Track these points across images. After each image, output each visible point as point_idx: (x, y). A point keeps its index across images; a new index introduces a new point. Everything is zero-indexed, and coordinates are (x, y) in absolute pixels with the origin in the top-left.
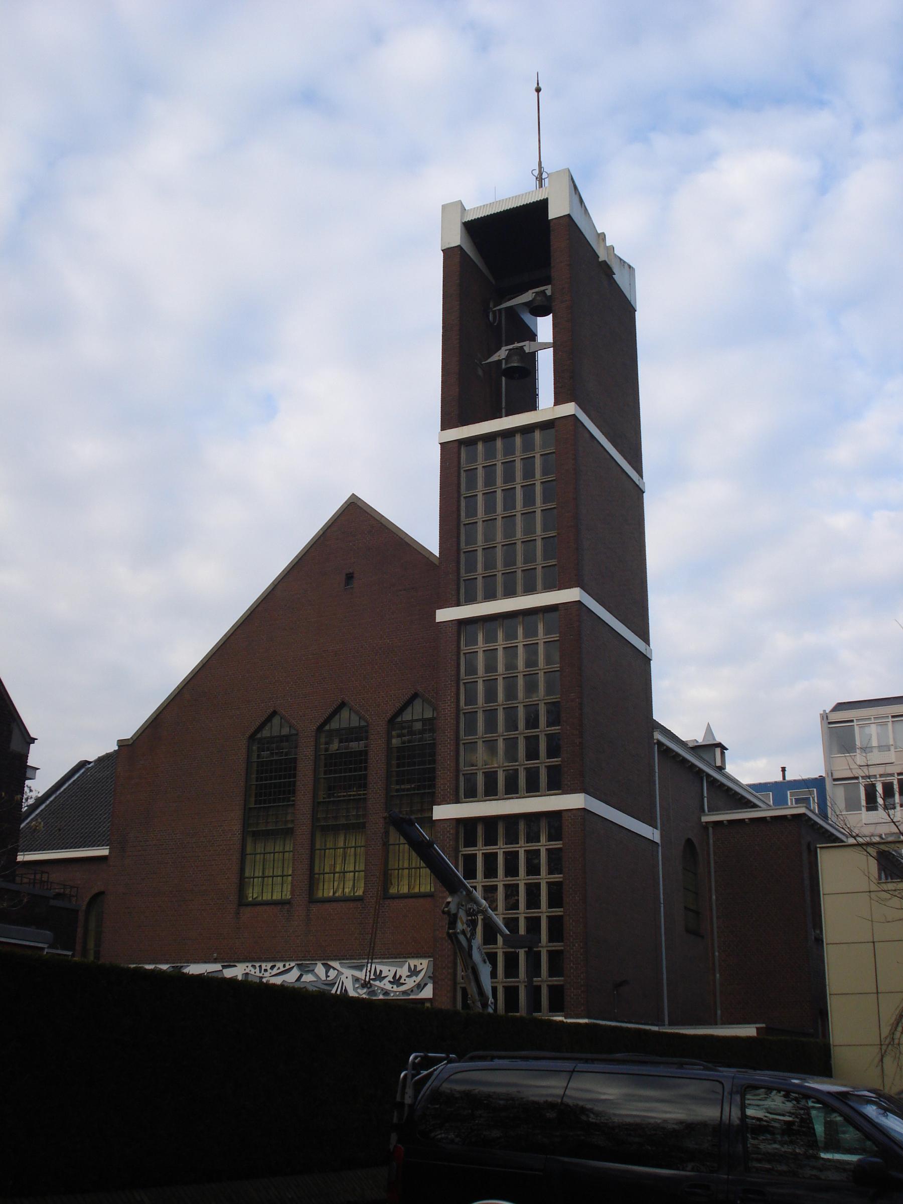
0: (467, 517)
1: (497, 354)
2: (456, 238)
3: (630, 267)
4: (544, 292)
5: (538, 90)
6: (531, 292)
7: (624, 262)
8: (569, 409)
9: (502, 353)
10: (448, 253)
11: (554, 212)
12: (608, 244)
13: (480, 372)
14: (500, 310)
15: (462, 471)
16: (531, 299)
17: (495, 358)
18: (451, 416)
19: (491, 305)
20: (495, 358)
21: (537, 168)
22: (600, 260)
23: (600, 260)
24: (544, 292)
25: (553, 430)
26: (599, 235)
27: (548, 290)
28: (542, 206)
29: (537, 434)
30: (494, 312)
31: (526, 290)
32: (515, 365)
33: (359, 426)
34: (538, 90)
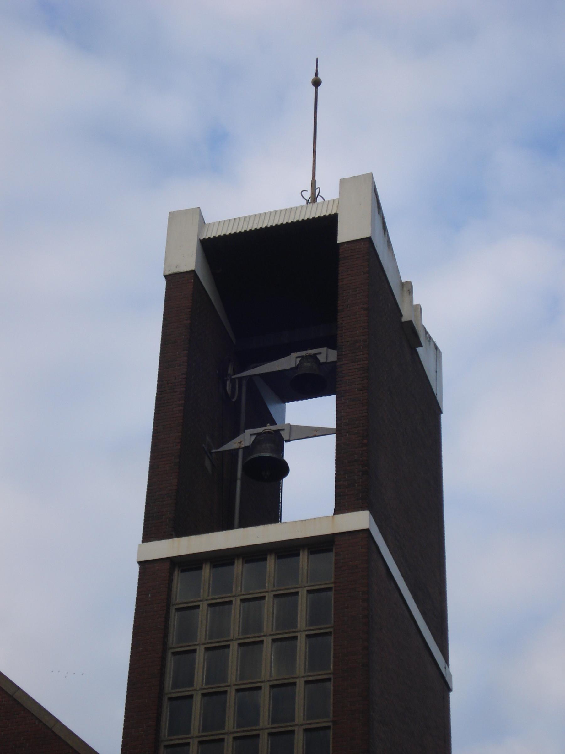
0: (175, 685)
1: (238, 439)
2: (189, 260)
3: (436, 348)
4: (314, 357)
5: (317, 83)
6: (294, 355)
7: (430, 338)
8: (360, 520)
9: (246, 438)
10: (172, 280)
11: (345, 234)
12: (415, 302)
13: (208, 464)
14: (240, 379)
15: (173, 611)
16: (293, 365)
17: (233, 445)
18: (156, 526)
19: (230, 371)
20: (233, 445)
21: (309, 188)
22: (404, 319)
23: (404, 319)
24: (314, 357)
25: (332, 556)
26: (403, 285)
27: (326, 355)
28: (330, 222)
29: (304, 558)
30: (233, 381)
31: (286, 353)
32: (268, 455)
33: (314, 76)
34: (317, 83)
